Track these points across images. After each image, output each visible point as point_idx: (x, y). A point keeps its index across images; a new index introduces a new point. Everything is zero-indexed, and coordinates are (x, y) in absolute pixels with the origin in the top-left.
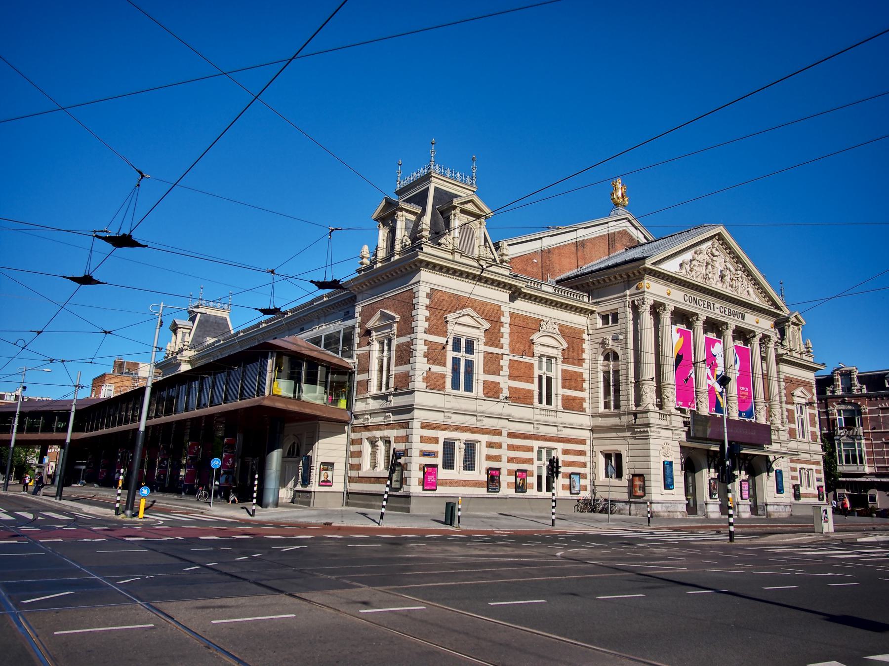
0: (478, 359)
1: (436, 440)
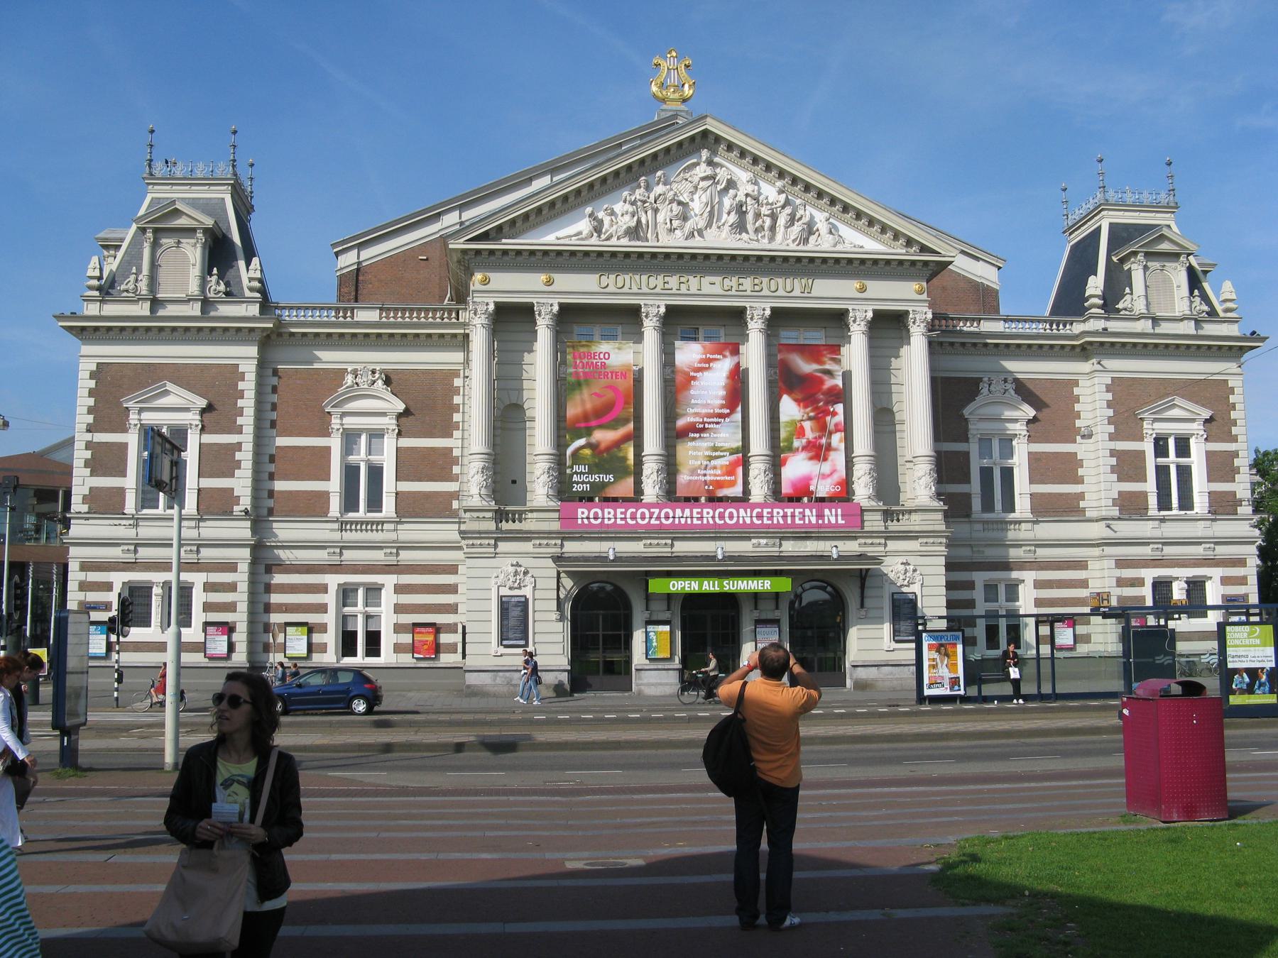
0: (1197, 461)
1: (1139, 582)
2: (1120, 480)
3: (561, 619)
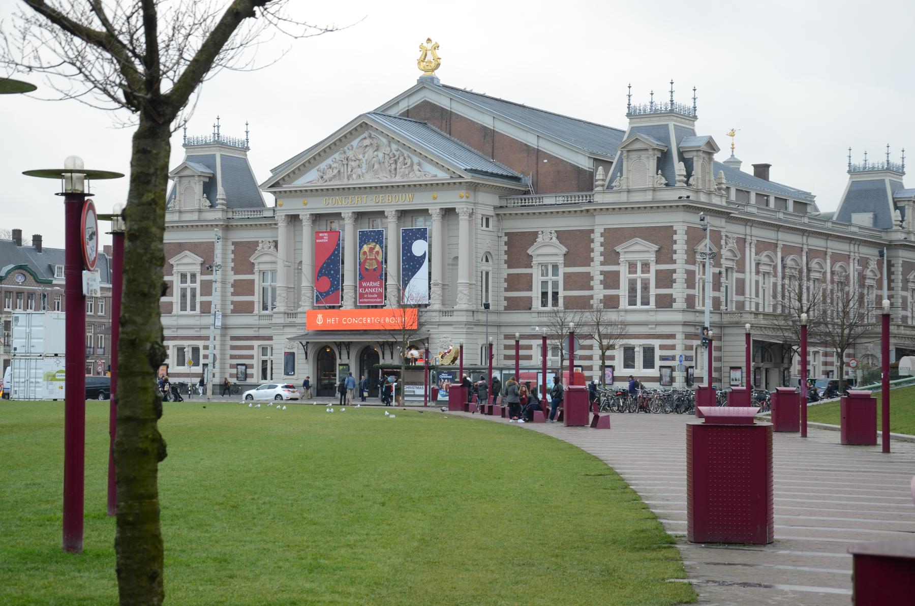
3: (307, 363)
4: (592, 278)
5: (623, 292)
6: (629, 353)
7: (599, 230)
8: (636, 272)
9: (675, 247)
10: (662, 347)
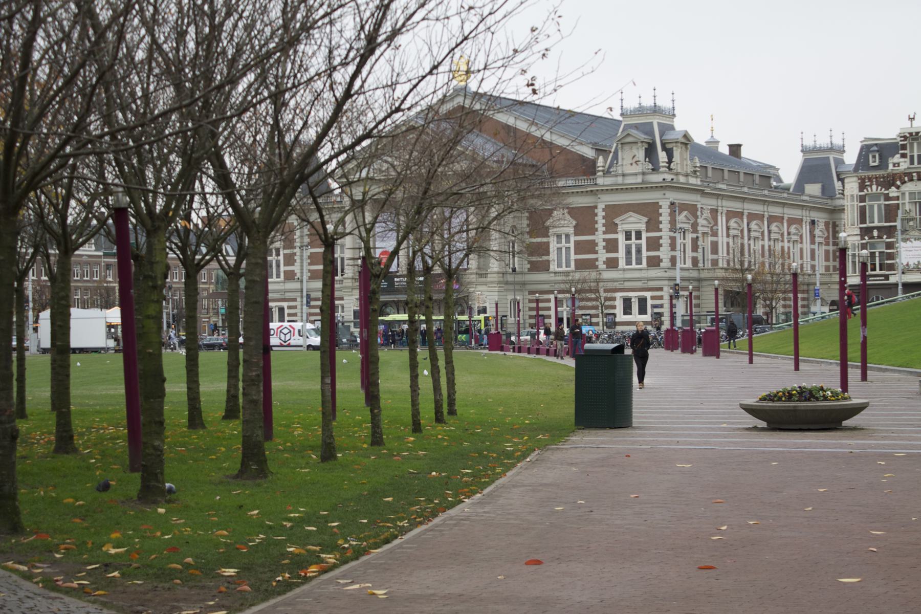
2: (607, 252)
4: (596, 245)
5: (621, 254)
6: (627, 303)
7: (601, 206)
8: (630, 239)
9: (661, 219)
10: (653, 298)
